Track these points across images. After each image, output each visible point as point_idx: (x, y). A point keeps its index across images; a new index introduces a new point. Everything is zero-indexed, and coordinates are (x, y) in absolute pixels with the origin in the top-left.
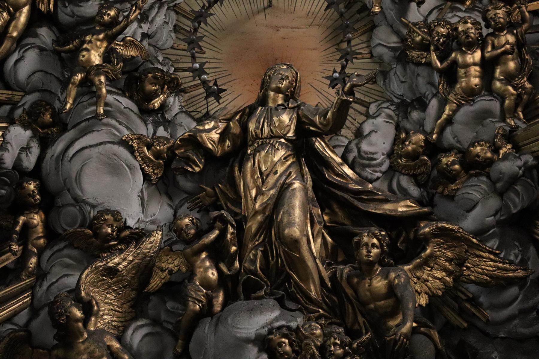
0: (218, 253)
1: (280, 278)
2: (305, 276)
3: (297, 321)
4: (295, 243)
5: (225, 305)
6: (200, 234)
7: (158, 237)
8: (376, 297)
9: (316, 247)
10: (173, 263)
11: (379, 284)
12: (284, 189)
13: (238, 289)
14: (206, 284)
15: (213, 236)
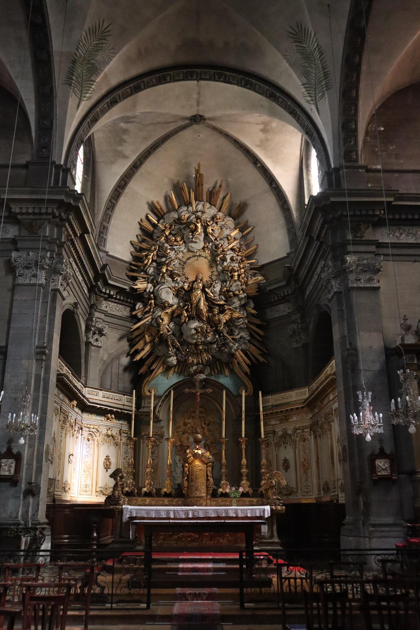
0: (187, 311)
1: (198, 316)
2: (203, 316)
3: (202, 325)
4: (202, 310)
5: (188, 321)
6: (184, 307)
7: (175, 306)
8: (216, 321)
9: (205, 310)
10: (179, 312)
11: (217, 318)
12: (200, 299)
13: (191, 318)
14: (185, 317)
15: (186, 307)
